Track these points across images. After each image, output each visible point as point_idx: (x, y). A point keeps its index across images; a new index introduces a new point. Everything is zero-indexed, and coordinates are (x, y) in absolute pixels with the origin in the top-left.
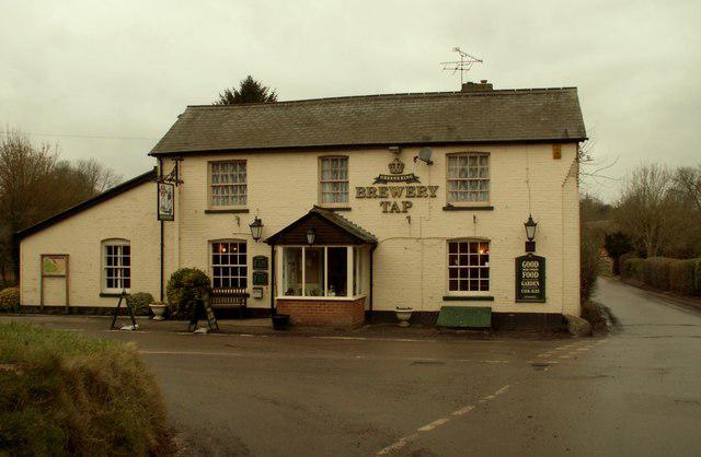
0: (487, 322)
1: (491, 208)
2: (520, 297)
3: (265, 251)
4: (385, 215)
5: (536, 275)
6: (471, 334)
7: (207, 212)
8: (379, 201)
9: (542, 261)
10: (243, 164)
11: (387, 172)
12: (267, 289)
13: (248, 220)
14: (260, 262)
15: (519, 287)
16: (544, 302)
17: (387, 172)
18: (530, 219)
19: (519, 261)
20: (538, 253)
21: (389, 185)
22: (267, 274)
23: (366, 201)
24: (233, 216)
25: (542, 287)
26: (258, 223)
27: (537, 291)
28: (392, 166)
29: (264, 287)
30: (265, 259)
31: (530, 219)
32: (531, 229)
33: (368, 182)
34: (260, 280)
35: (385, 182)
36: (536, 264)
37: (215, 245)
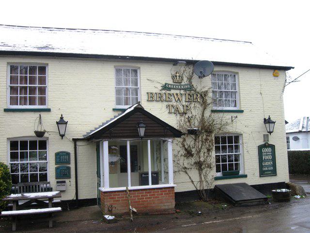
0: (171, 204)
1: (242, 111)
2: (262, 173)
3: (69, 148)
4: (170, 115)
5: (270, 157)
6: (157, 212)
7: (6, 110)
8: (166, 103)
9: (273, 147)
10: (43, 70)
11: (170, 82)
12: (70, 183)
13: (53, 118)
14: (61, 158)
15: (261, 166)
16: (276, 175)
17: (170, 82)
18: (62, 118)
19: (260, 148)
20: (270, 142)
21: (172, 91)
22: (69, 168)
23: (154, 103)
24: (37, 115)
25: (274, 165)
26: (62, 122)
27: (272, 168)
28: (173, 77)
29: (67, 181)
30: (68, 154)
31: (62, 118)
32: (62, 127)
33: (156, 89)
34: (63, 174)
35: (170, 89)
36: (270, 150)
37: (14, 144)
